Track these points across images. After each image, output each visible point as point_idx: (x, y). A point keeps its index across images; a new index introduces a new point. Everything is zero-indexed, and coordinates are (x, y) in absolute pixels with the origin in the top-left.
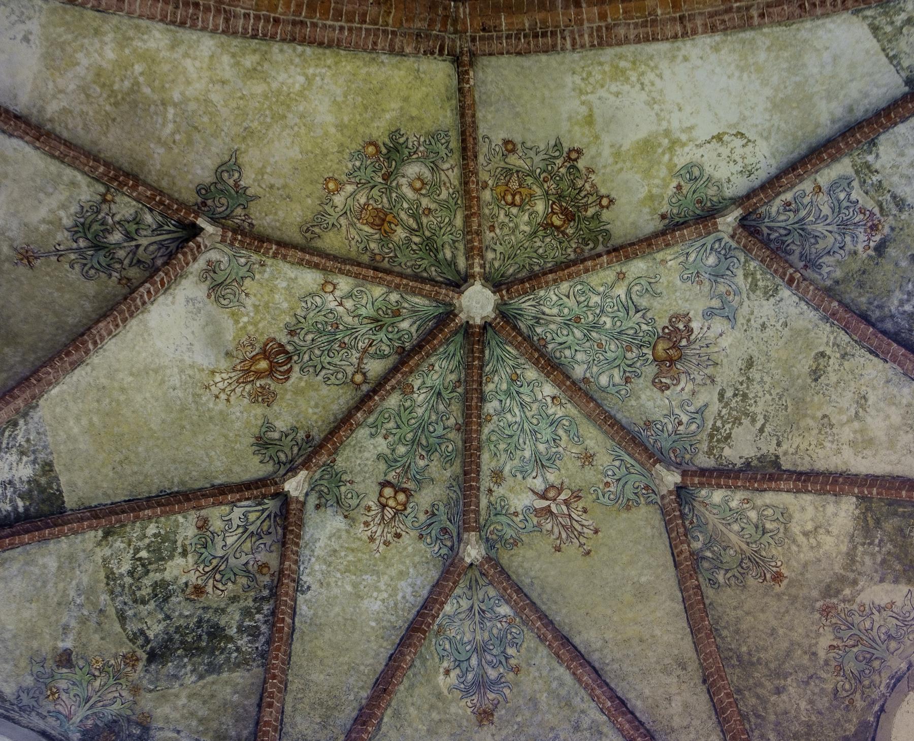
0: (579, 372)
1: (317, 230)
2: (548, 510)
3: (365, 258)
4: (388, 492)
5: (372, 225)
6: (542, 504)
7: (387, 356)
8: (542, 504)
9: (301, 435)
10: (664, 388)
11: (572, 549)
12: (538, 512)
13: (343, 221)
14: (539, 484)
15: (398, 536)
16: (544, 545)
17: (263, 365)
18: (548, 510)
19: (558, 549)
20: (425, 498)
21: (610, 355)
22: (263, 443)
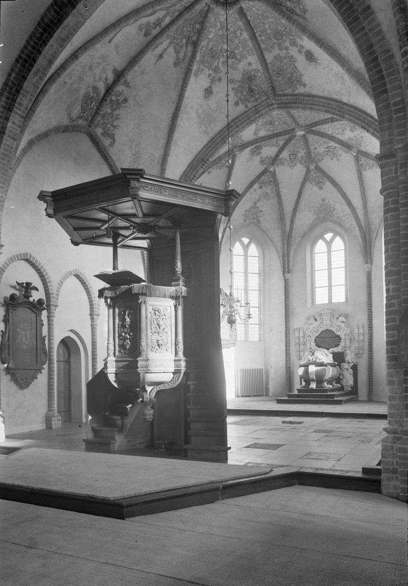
0: (330, 133)
1: (257, 132)
2: (329, 151)
3: (270, 133)
4: (291, 156)
5: (269, 125)
6: (326, 150)
7: (283, 140)
8: (326, 150)
9: (269, 157)
10: (353, 131)
11: (335, 159)
12: (326, 151)
13: (262, 127)
14: (326, 146)
15: (296, 164)
16: (329, 158)
17: (256, 149)
18: (329, 151)
19: (332, 159)
20: (300, 155)
21: (338, 127)
22: (262, 162)
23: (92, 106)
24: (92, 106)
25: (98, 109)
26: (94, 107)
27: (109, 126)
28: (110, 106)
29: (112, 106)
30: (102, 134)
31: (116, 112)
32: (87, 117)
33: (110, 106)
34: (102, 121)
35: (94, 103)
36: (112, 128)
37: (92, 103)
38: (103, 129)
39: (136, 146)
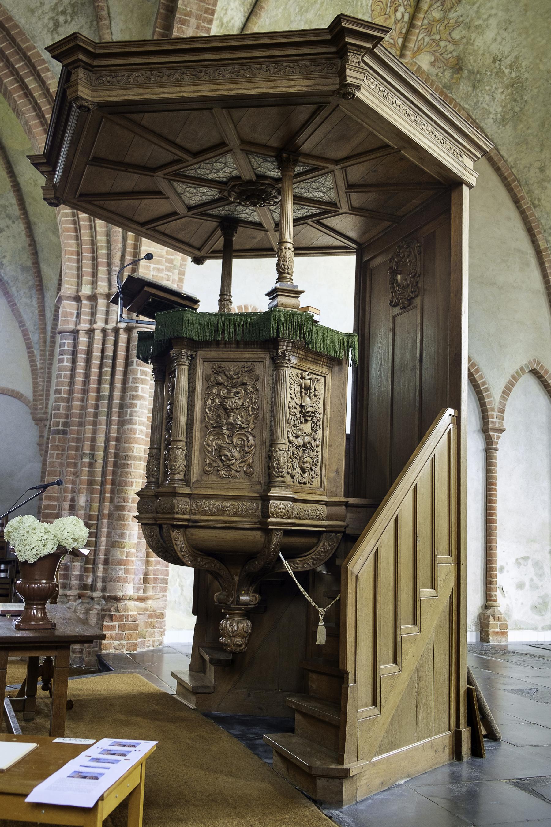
23: (399, 15)
24: (399, 15)
25: (413, 17)
26: (403, 17)
27: (442, 44)
28: (439, 4)
29: (443, 4)
30: (433, 64)
31: (452, 15)
32: (392, 41)
33: (439, 4)
34: (427, 39)
35: (401, 9)
36: (450, 47)
37: (396, 10)
38: (433, 53)
39: (511, 66)
